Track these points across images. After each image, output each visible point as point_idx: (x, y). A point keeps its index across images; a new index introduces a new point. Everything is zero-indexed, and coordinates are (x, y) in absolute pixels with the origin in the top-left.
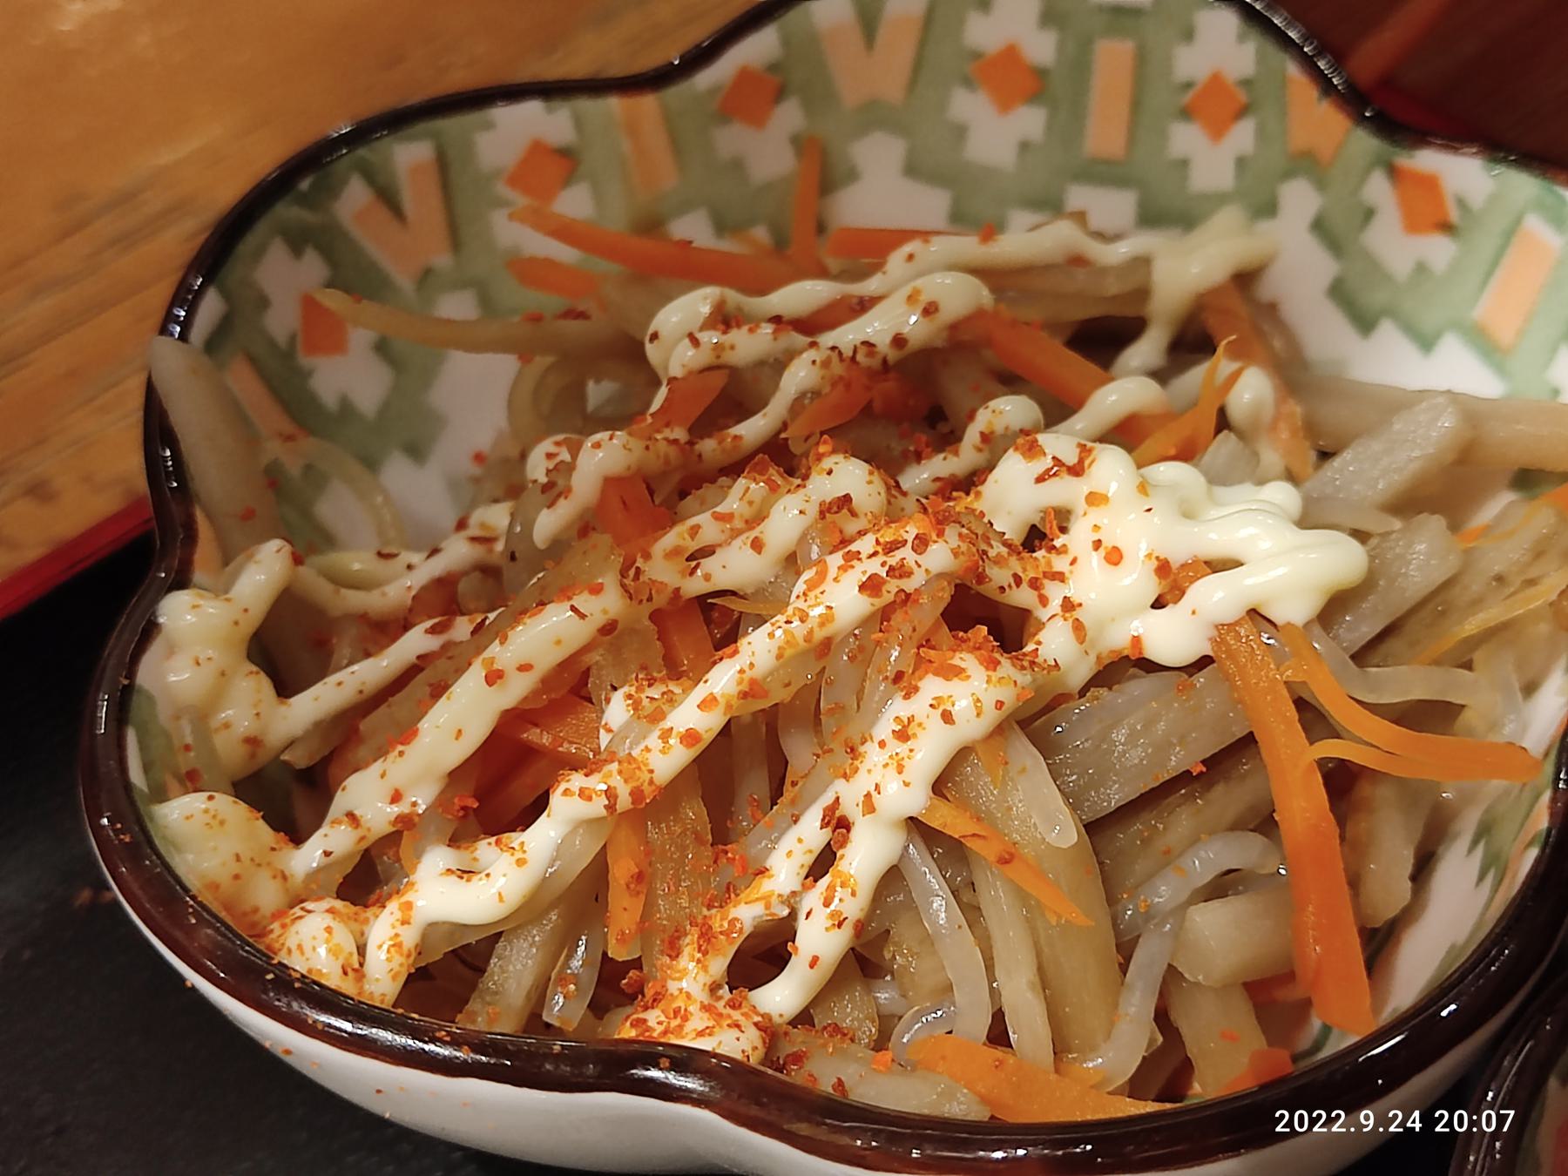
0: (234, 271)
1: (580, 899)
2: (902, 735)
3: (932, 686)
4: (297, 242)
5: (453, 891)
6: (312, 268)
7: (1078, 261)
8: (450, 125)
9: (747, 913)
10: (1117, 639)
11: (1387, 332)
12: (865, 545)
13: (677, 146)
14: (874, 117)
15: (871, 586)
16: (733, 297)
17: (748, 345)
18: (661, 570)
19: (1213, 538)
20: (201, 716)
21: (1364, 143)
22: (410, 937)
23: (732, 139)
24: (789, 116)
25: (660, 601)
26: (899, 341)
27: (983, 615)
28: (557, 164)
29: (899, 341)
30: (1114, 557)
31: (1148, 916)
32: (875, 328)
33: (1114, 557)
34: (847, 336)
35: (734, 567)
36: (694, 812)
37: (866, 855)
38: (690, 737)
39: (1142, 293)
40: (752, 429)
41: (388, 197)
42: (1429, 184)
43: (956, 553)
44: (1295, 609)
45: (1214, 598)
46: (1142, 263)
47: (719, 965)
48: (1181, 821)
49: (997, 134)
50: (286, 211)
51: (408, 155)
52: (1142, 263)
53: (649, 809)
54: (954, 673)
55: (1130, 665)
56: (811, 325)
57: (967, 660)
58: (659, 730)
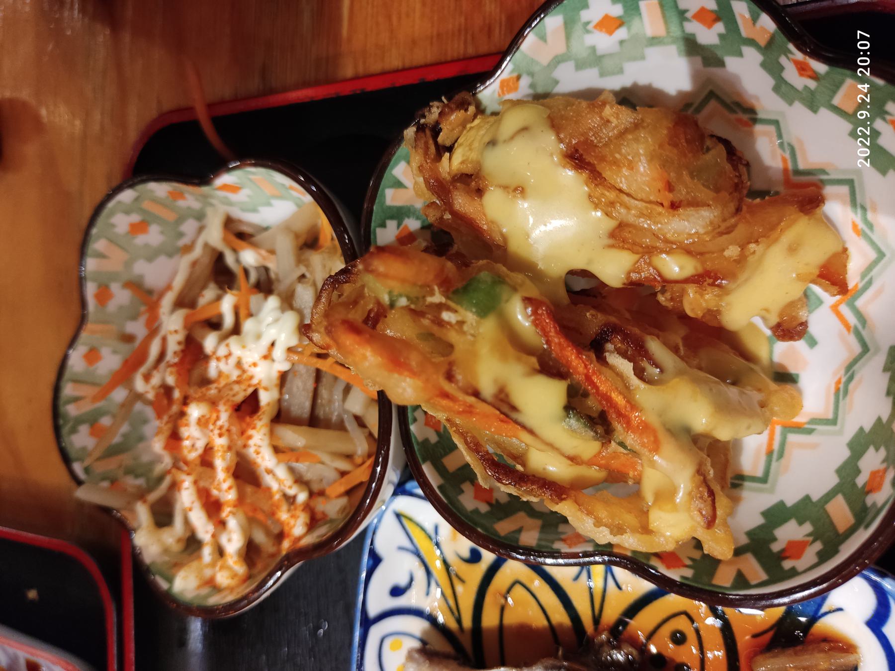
0: (72, 454)
1: (251, 521)
2: (258, 453)
3: (251, 442)
4: (74, 430)
5: (233, 542)
6: (84, 429)
7: (194, 264)
8: (67, 375)
9: (277, 497)
10: (275, 375)
11: (261, 209)
12: (211, 427)
13: (105, 322)
14: (128, 264)
15: (220, 435)
16: (143, 369)
17: (156, 380)
18: (193, 456)
19: (265, 342)
20: (166, 551)
21: (205, 189)
22: (235, 558)
23: (112, 306)
24: (115, 288)
25: (198, 462)
26: (179, 343)
27: (248, 406)
28: (92, 356)
29: (179, 343)
30: (255, 365)
31: (339, 415)
32: (173, 346)
33: (255, 365)
34: (170, 357)
35: (201, 445)
36: (249, 489)
37: (281, 472)
38: (230, 488)
39: (214, 250)
40: (177, 394)
41: (76, 400)
42: (225, 187)
43: (226, 411)
44: (294, 341)
45: (279, 353)
46: (206, 245)
47: (284, 507)
48: (324, 393)
49: (154, 236)
50: (65, 430)
51: (68, 390)
52: (206, 245)
53: (241, 501)
54: (250, 437)
55: (283, 378)
56: (162, 355)
57: (251, 432)
58: (225, 489)
